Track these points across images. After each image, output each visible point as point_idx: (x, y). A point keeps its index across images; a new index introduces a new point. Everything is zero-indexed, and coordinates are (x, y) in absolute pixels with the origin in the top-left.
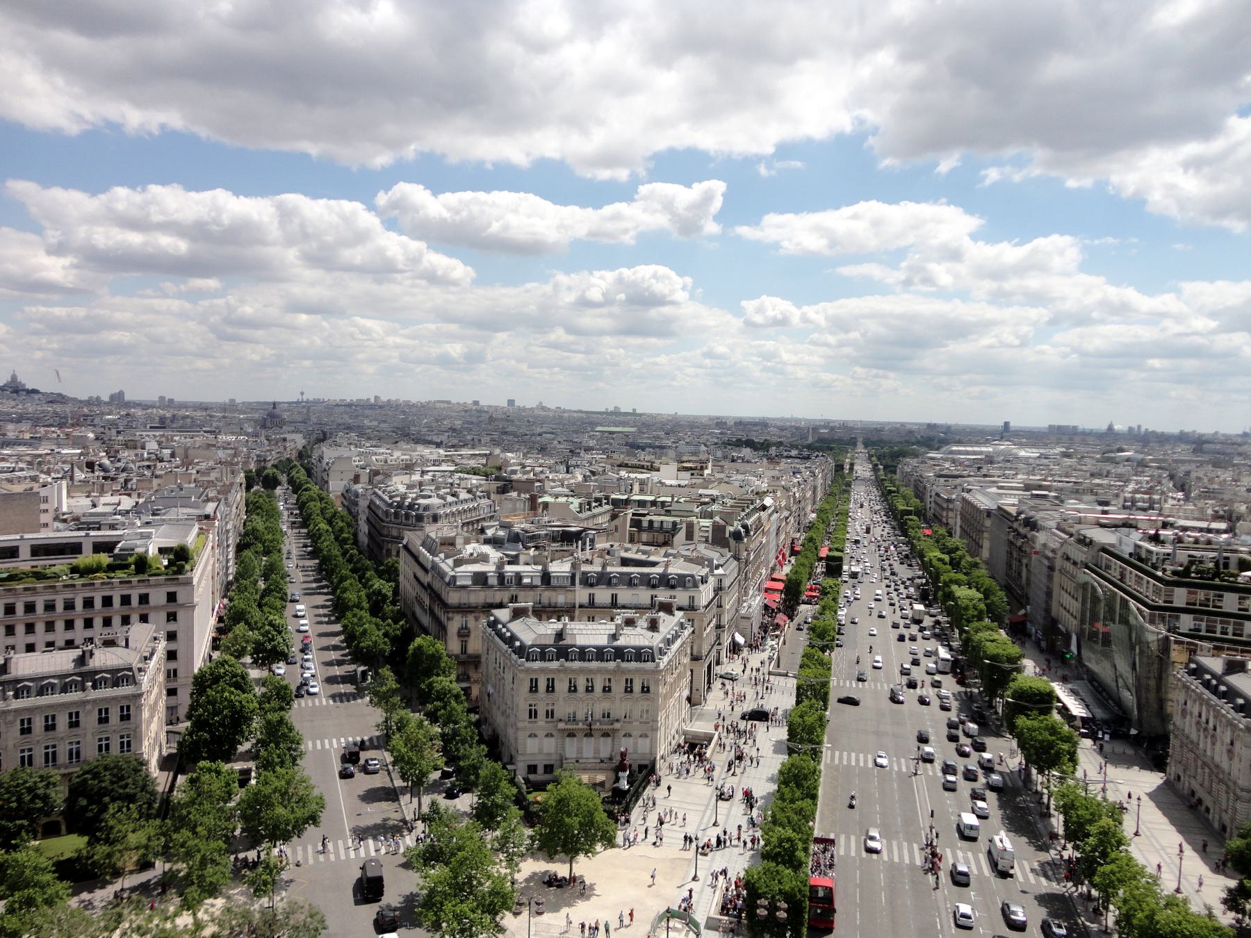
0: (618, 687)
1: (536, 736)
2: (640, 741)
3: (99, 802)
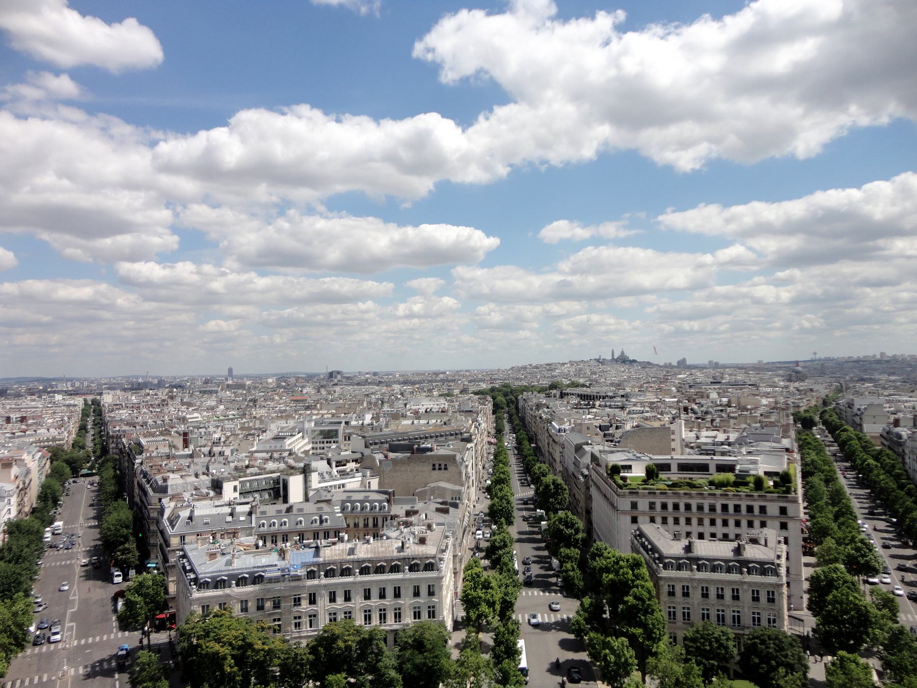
3: (768, 663)
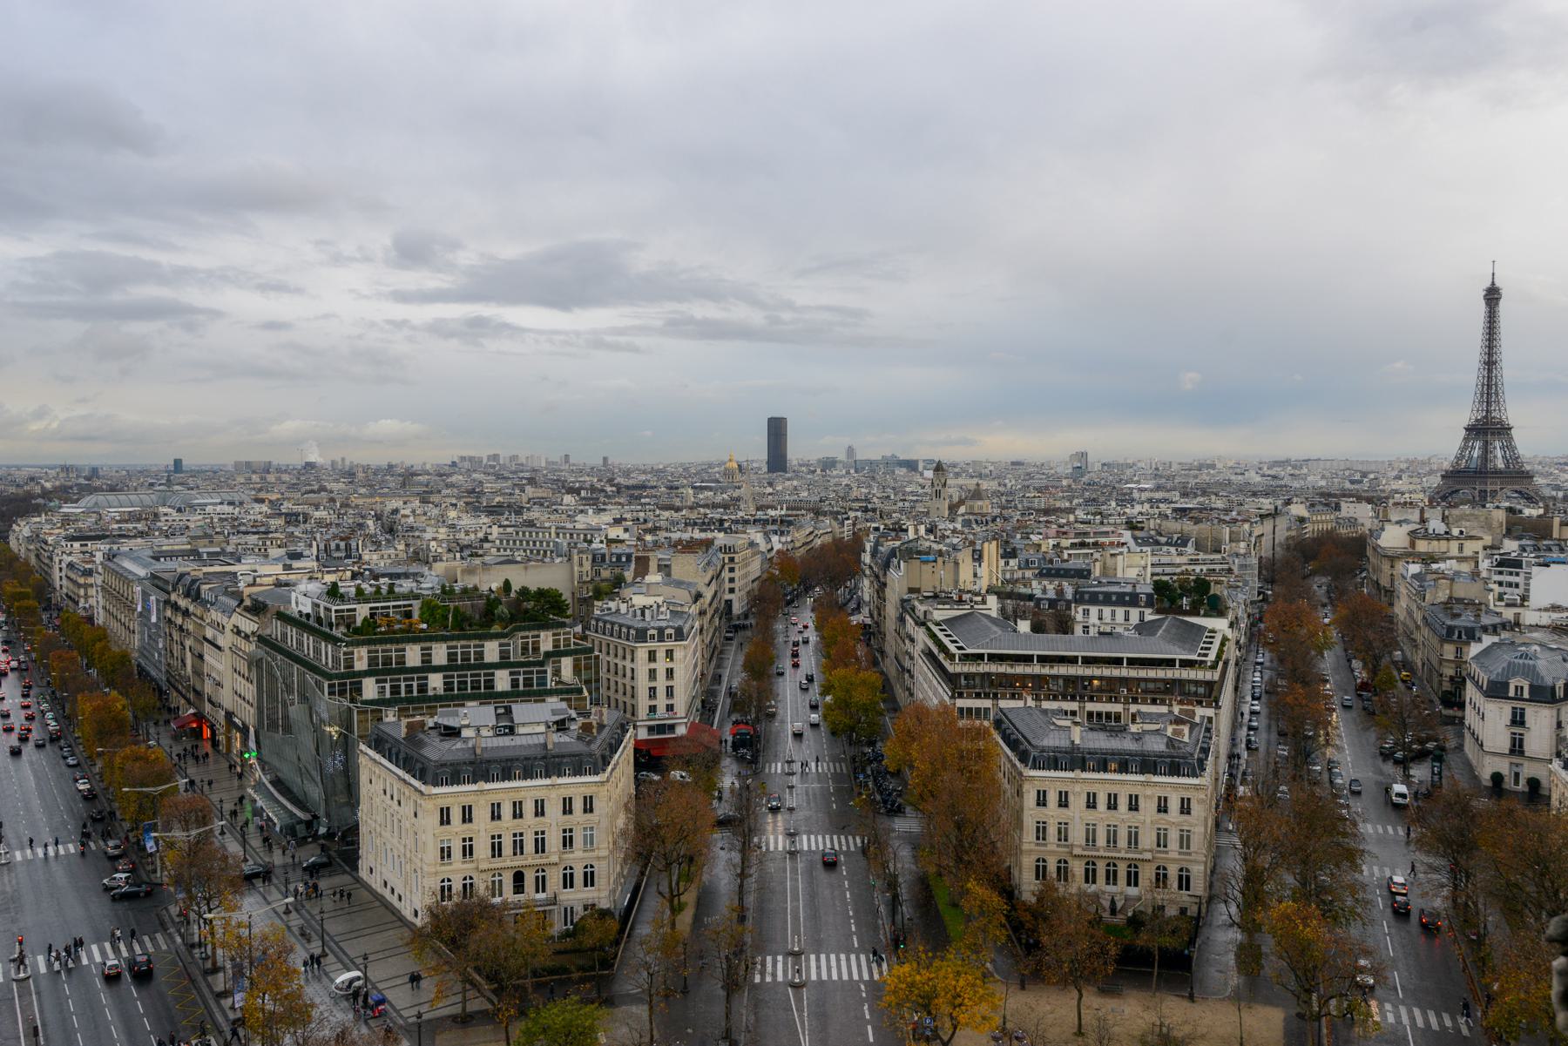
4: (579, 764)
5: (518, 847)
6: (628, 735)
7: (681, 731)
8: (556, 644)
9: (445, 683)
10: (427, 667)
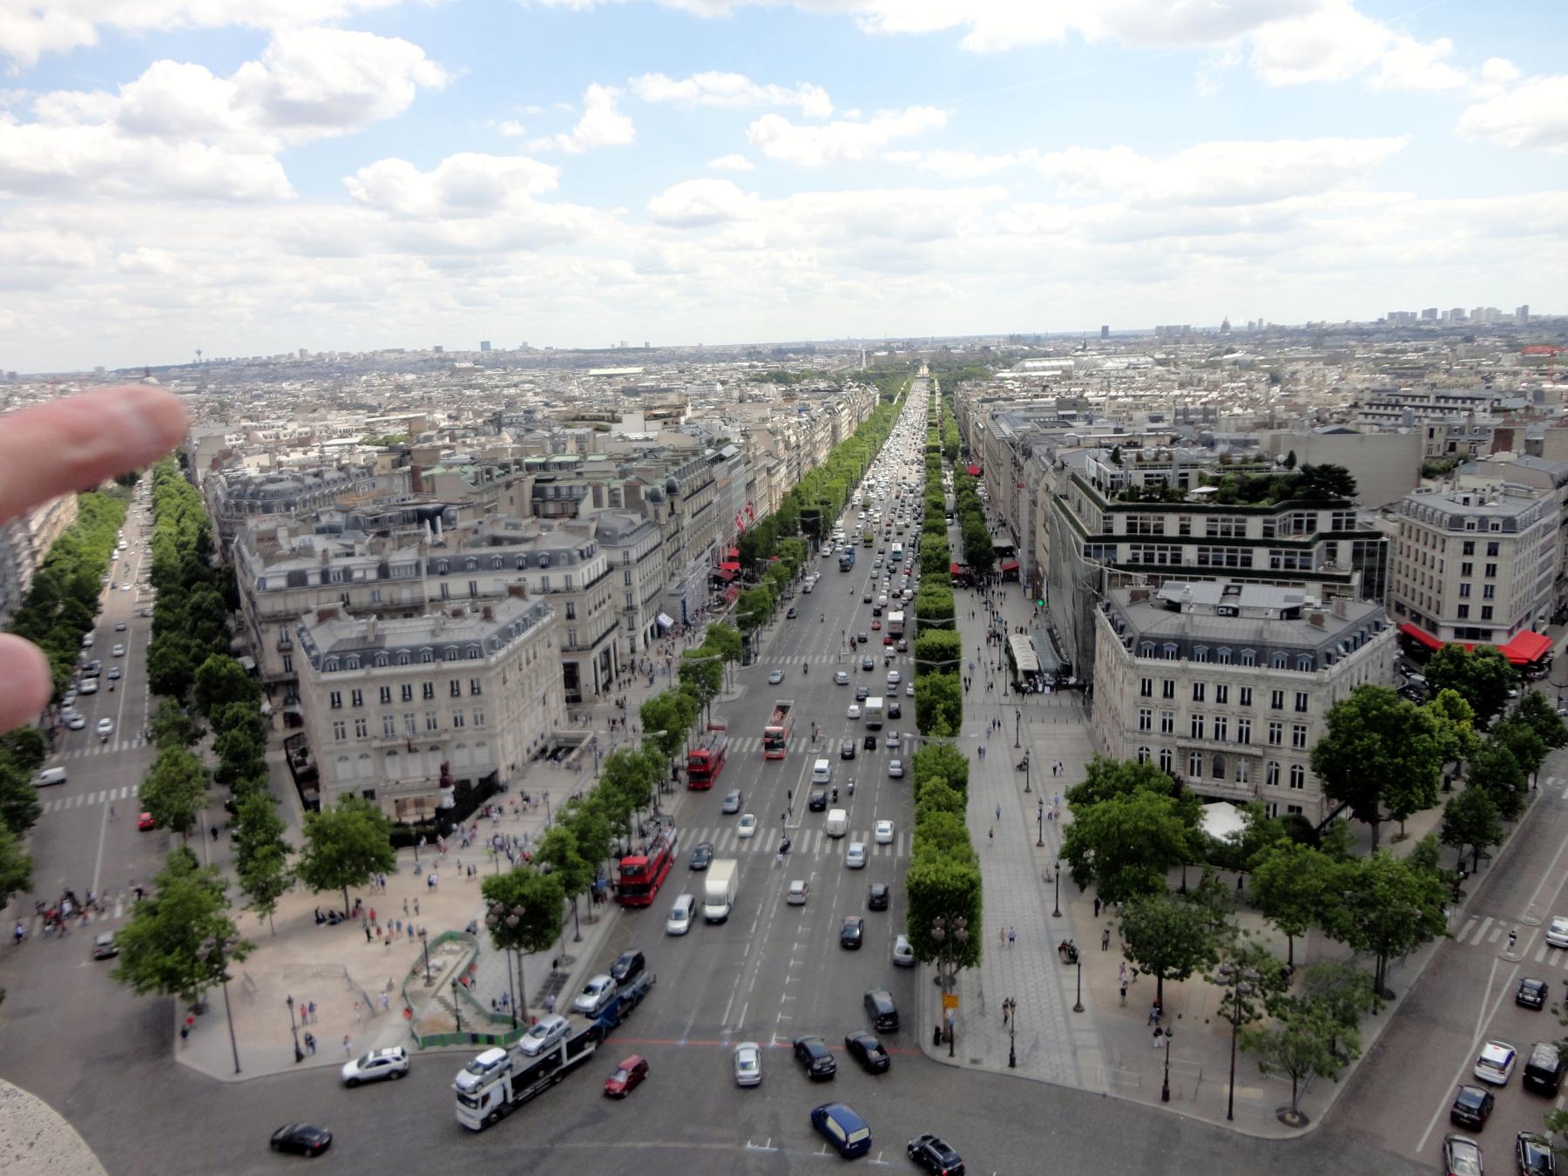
0: (442, 691)
1: (347, 759)
2: (477, 751)
4: (1293, 658)
5: (1220, 731)
6: (1383, 636)
7: (1500, 640)
8: (1336, 525)
9: (1200, 556)
10: (1185, 537)
